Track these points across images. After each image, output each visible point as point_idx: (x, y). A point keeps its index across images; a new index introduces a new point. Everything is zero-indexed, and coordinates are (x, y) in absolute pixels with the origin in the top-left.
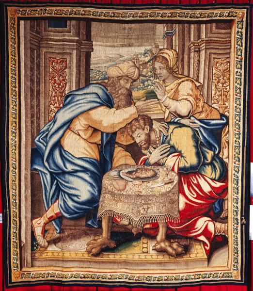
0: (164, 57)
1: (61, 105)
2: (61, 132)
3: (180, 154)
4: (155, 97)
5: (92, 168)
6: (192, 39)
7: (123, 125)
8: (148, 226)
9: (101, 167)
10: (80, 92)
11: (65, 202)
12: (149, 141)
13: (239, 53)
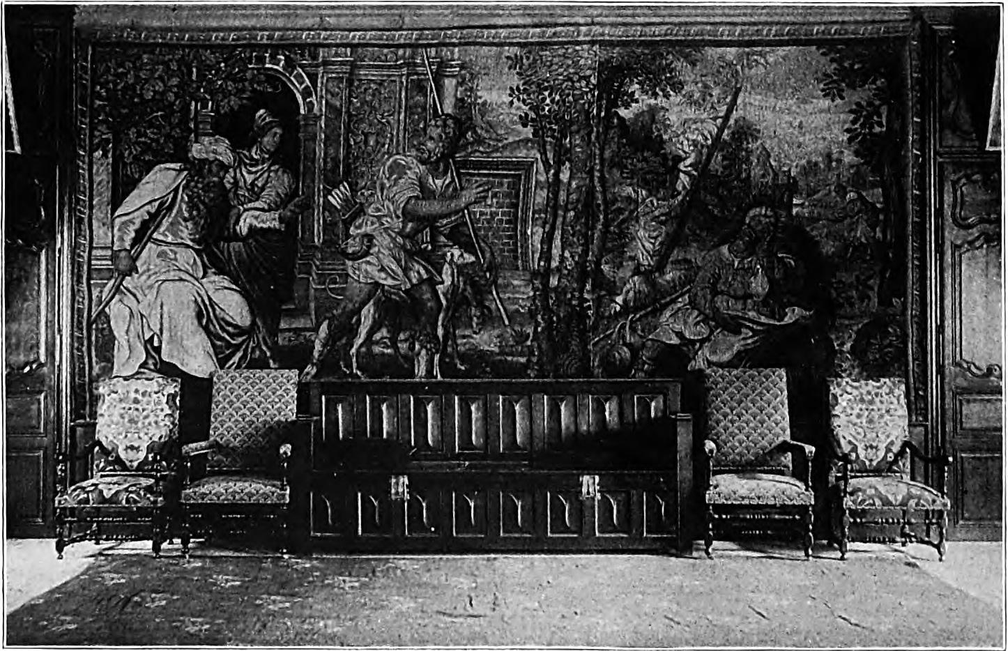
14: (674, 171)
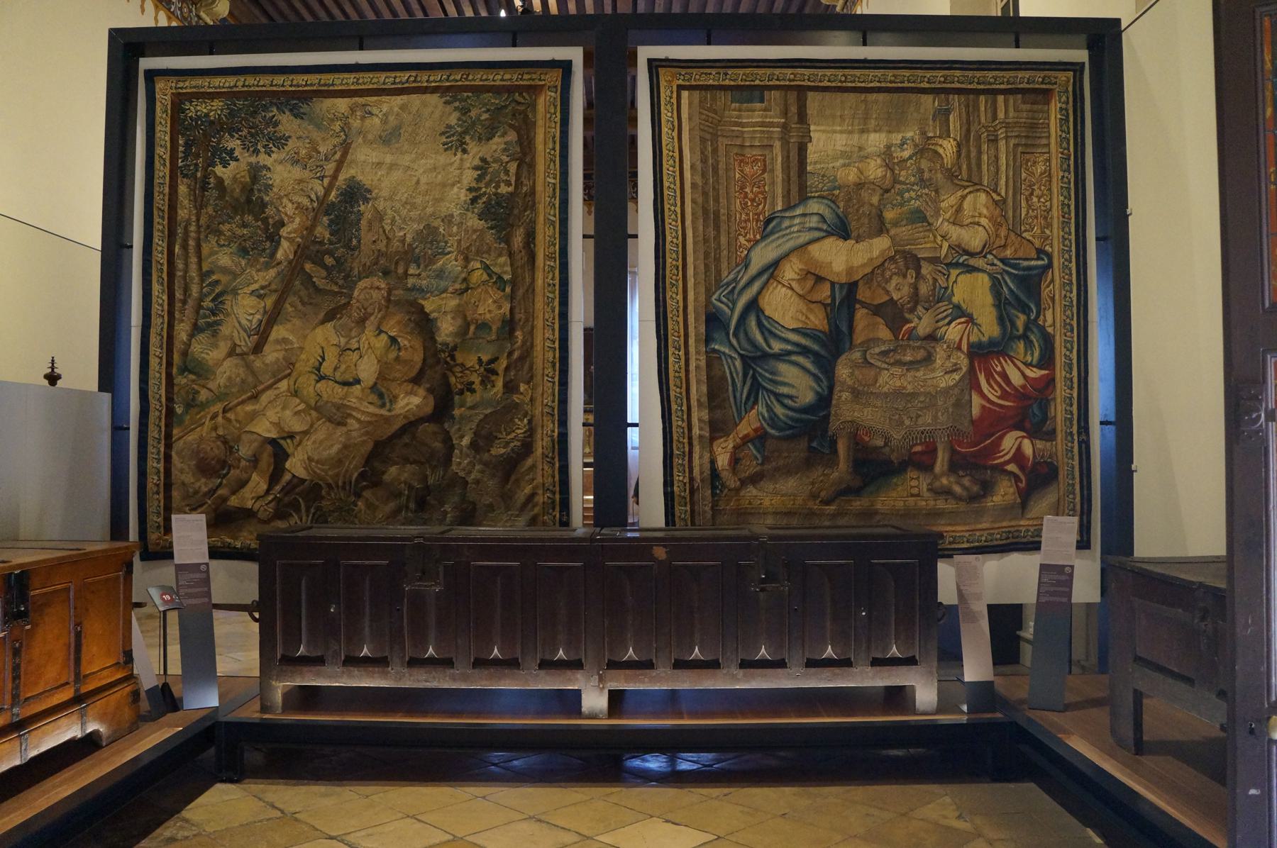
0: (936, 152)
1: (758, 237)
2: (756, 286)
3: (971, 319)
4: (924, 219)
5: (816, 347)
6: (983, 120)
7: (868, 270)
8: (918, 448)
9: (828, 346)
10: (787, 214)
11: (770, 409)
12: (915, 298)
13: (1065, 145)
14: (274, 239)
